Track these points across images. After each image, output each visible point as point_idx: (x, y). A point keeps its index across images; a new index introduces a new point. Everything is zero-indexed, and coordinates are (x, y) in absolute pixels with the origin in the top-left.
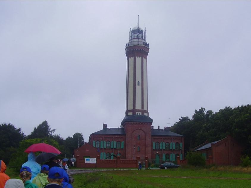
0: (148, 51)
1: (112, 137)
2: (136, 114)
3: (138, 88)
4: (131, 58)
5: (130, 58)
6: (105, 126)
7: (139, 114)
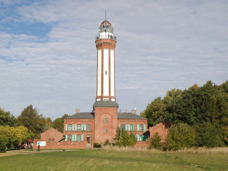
2: (104, 100)
3: (106, 78)
7: (106, 100)
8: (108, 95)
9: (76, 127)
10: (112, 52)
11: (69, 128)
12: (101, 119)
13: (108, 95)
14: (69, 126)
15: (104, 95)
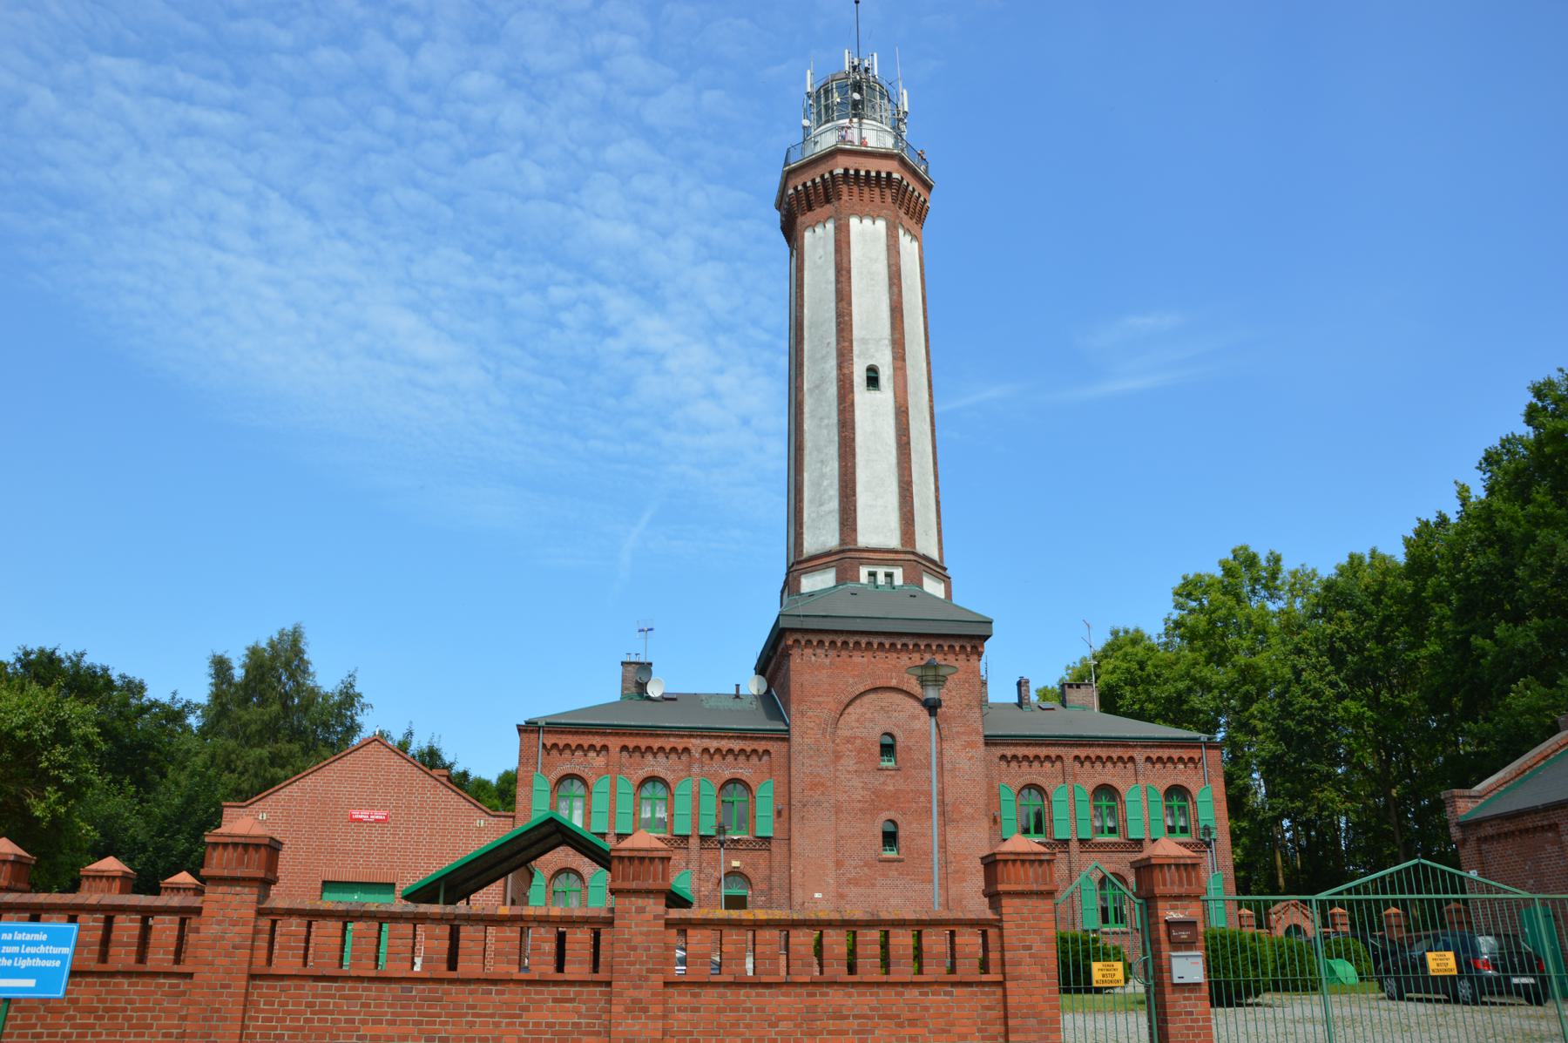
1: (686, 750)
4: (819, 230)
5: (808, 235)
6: (638, 673)
7: (881, 579)
8: (894, 542)
10: (909, 248)
12: (848, 733)
13: (894, 542)
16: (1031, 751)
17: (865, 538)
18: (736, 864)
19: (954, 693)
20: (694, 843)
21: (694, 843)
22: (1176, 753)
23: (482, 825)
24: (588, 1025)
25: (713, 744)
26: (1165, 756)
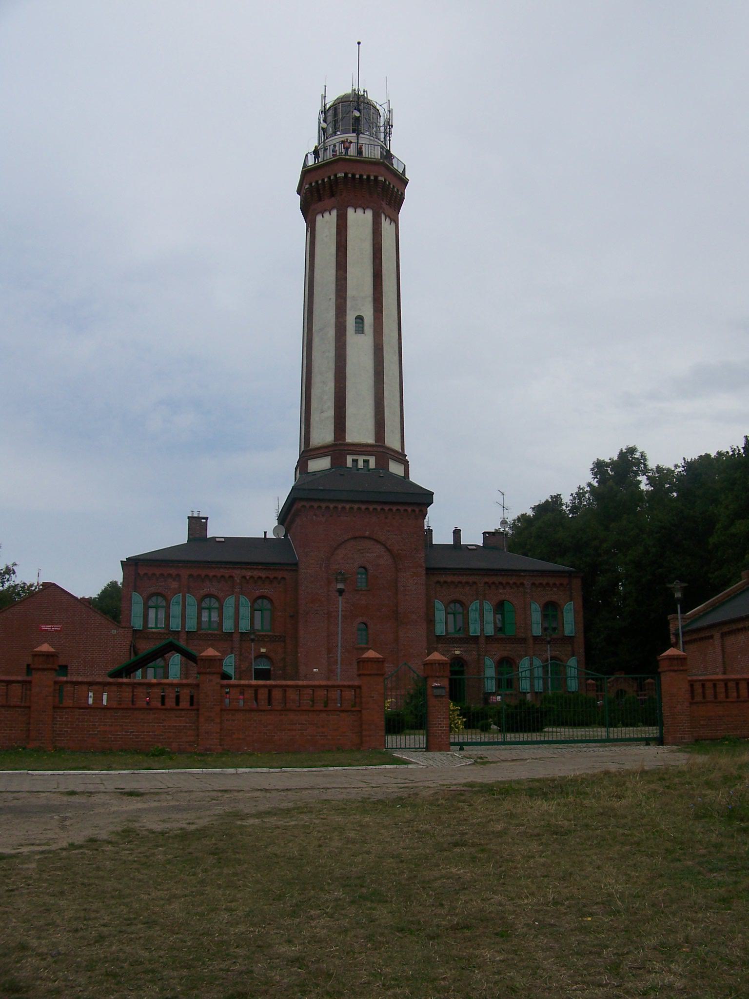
0: (403, 194)
1: (231, 577)
2: (349, 463)
4: (326, 215)
5: (319, 218)
6: (197, 524)
7: (361, 464)
9: (192, 611)
11: (152, 613)
13: (371, 440)
14: (153, 602)
15: (349, 439)
16: (456, 579)
17: (352, 437)
18: (263, 650)
19: (406, 541)
20: (236, 638)
21: (236, 638)
22: (552, 581)
23: (115, 633)
24: (190, 726)
25: (249, 574)
26: (544, 582)
